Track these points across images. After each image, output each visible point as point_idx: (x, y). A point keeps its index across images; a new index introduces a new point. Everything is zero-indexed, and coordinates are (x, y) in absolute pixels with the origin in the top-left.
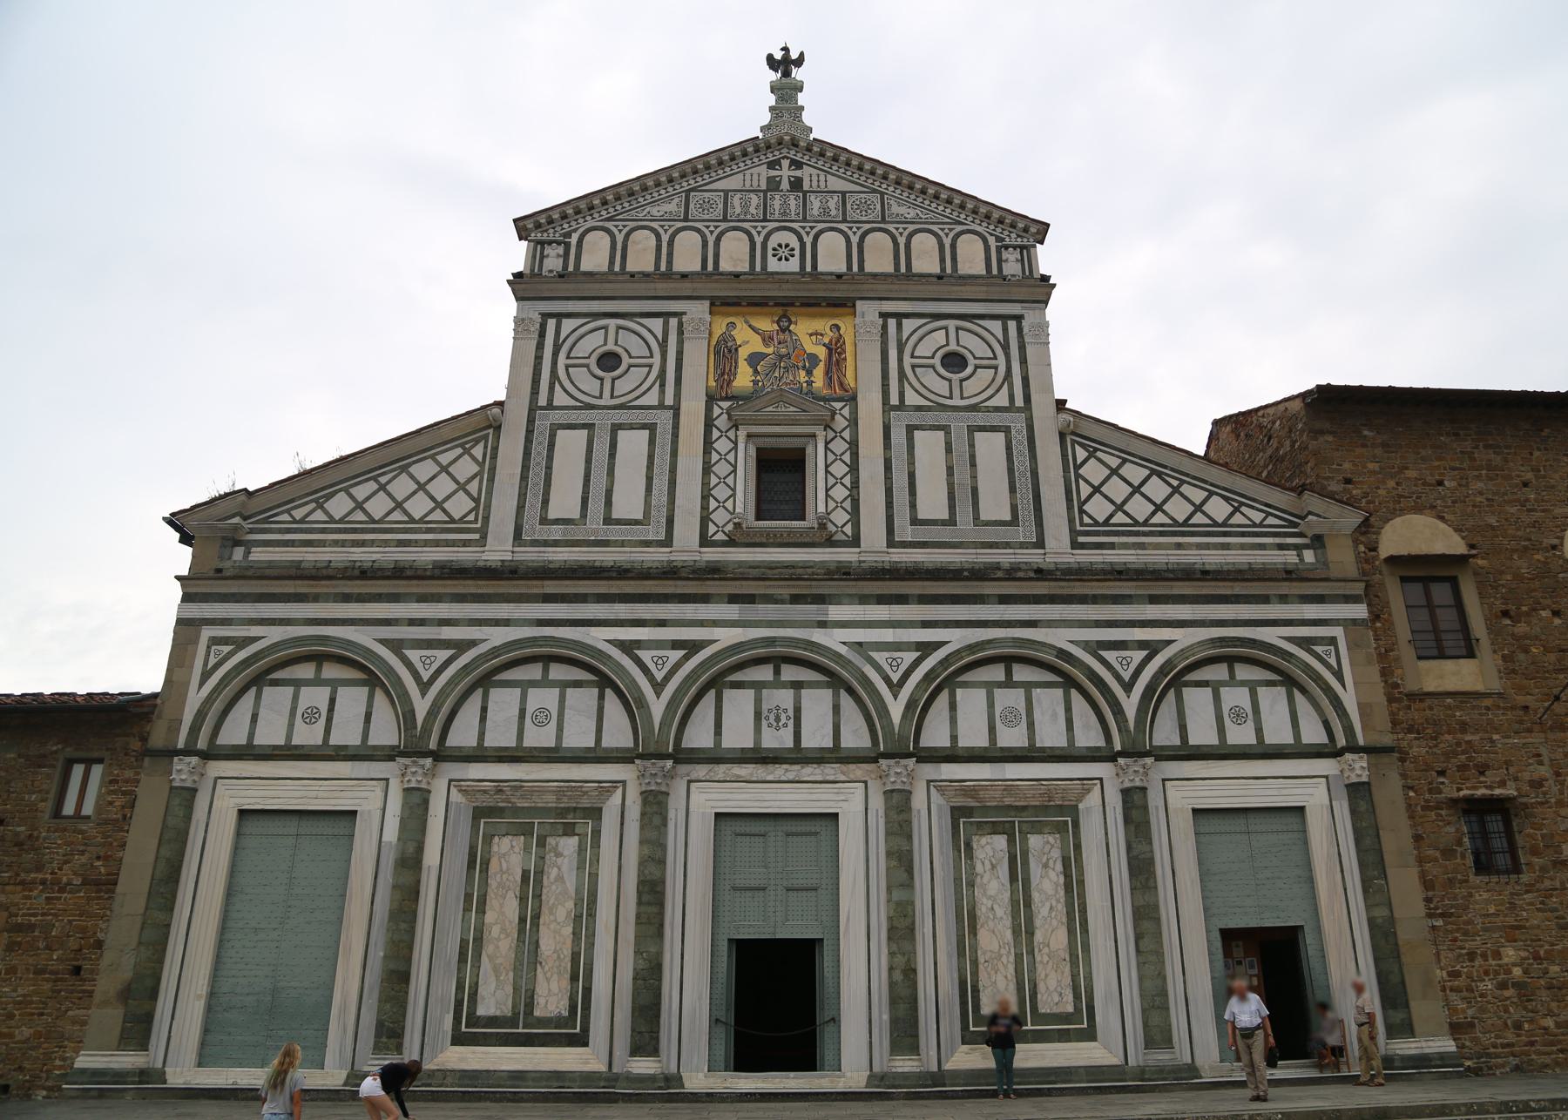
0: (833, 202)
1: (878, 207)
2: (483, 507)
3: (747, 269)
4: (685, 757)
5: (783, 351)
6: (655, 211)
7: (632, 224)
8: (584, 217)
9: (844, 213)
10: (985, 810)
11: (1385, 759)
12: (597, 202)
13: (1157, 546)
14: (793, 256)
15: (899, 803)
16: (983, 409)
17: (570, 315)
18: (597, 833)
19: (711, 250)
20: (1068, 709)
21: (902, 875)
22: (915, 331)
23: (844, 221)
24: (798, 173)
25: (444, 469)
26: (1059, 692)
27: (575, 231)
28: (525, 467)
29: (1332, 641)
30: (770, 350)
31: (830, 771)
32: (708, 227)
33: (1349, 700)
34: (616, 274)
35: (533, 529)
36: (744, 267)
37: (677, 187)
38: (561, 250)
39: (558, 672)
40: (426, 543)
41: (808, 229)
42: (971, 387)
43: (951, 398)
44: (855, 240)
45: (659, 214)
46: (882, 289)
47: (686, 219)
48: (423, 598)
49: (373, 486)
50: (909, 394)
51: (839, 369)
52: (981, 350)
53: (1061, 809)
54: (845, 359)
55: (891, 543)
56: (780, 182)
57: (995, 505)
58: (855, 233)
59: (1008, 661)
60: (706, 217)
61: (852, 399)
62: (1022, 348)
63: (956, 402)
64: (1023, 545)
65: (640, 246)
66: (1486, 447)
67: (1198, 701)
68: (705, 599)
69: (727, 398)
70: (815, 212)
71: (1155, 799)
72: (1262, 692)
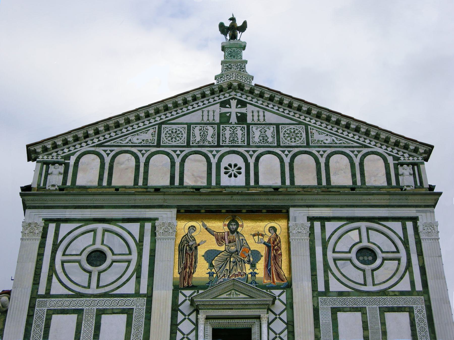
0: (270, 131)
1: (304, 135)
3: (205, 184)
5: (233, 249)
6: (135, 139)
7: (117, 149)
8: (80, 144)
9: (278, 141)
12: (91, 132)
14: (240, 173)
16: (391, 294)
22: (335, 231)
23: (279, 146)
24: (243, 110)
27: (73, 154)
30: (222, 248)
32: (175, 151)
34: (104, 187)
36: (203, 182)
37: (152, 121)
38: (61, 169)
41: (251, 153)
42: (381, 275)
43: (365, 284)
44: (287, 160)
45: (138, 141)
46: (309, 199)
47: (158, 145)
51: (276, 263)
52: (387, 246)
54: (281, 254)
56: (230, 116)
58: (287, 155)
60: (174, 144)
65: (123, 166)
70: (257, 139)
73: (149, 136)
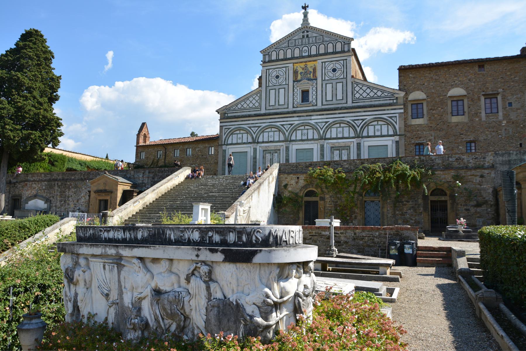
0: (314, 39)
2: (260, 104)
4: (291, 141)
6: (283, 46)
10: (336, 147)
11: (402, 136)
13: (367, 102)
15: (322, 147)
17: (271, 69)
18: (280, 153)
19: (293, 52)
20: (349, 131)
21: (322, 157)
24: (308, 34)
25: (254, 99)
26: (348, 128)
28: (266, 97)
29: (396, 117)
31: (312, 142)
33: (397, 127)
35: (268, 108)
39: (273, 129)
40: (253, 111)
42: (337, 75)
44: (318, 47)
48: (253, 120)
49: (244, 102)
50: (326, 77)
52: (339, 67)
53: (348, 146)
55: (322, 105)
57: (340, 97)
59: (340, 123)
61: (316, 79)
62: (346, 66)
63: (334, 78)
64: (344, 103)
66: (436, 75)
67: (371, 128)
68: (293, 117)
69: (297, 81)
71: (362, 144)
72: (382, 126)
73: (286, 45)
